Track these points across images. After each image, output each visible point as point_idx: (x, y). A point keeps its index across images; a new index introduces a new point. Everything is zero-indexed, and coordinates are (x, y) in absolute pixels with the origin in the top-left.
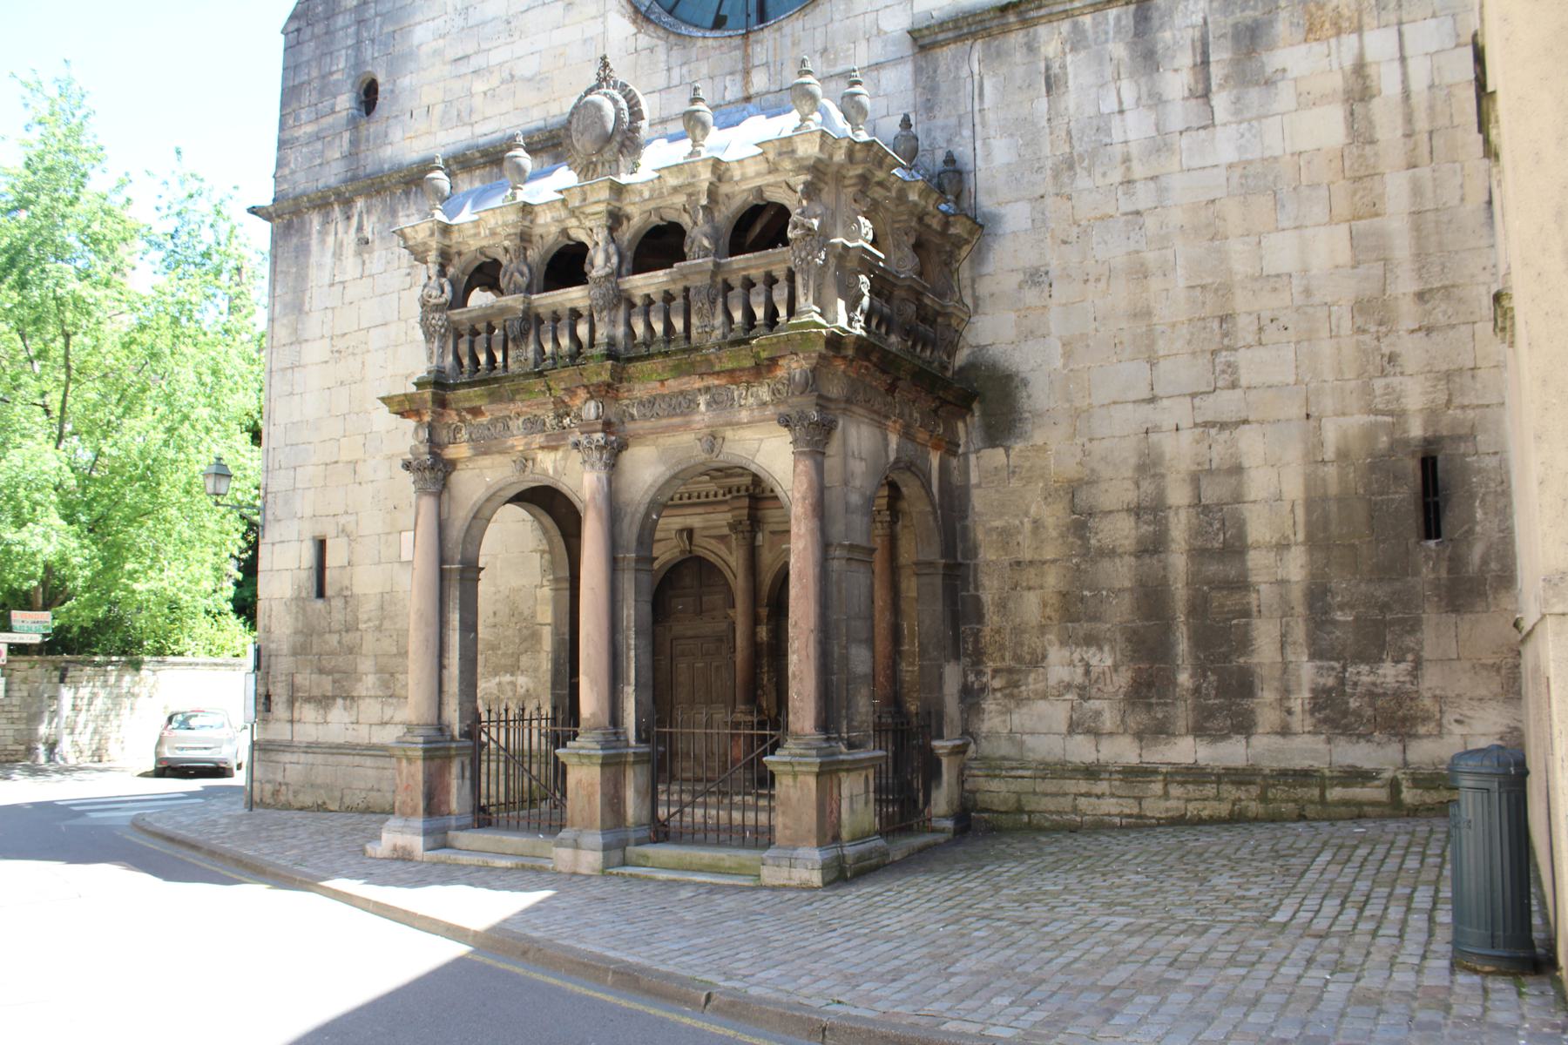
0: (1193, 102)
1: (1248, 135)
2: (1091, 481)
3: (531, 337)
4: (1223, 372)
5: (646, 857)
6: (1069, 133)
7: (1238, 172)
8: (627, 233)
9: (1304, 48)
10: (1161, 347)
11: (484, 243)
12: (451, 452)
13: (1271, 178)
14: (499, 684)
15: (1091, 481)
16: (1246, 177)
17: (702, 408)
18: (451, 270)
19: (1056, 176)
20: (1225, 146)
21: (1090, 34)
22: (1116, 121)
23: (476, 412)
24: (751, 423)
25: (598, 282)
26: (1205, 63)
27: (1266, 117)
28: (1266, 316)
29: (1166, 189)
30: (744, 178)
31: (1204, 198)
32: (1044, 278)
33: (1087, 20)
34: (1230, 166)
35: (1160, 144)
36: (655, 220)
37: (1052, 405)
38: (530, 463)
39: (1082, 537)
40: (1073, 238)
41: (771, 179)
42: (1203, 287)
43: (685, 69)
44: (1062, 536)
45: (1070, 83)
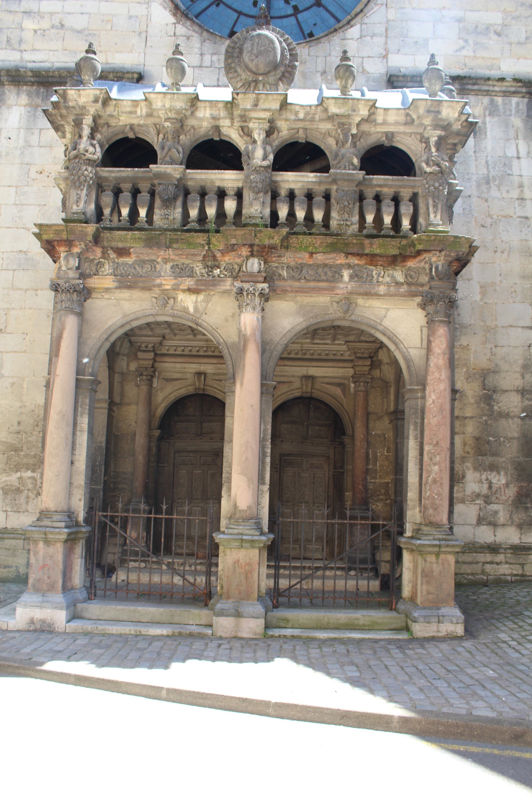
2: (495, 371)
5: (287, 620)
6: (487, 162)
8: (278, 140)
11: (135, 122)
12: (94, 282)
14: (20, 478)
15: (495, 371)
17: (346, 278)
18: (98, 136)
19: (479, 186)
21: (501, 108)
22: (515, 162)
23: (122, 252)
24: (388, 295)
25: (257, 170)
30: (385, 123)
33: (499, 100)
36: (301, 137)
37: (473, 322)
38: (172, 301)
39: (489, 405)
40: (488, 224)
41: (402, 129)
44: (477, 403)
45: (488, 134)
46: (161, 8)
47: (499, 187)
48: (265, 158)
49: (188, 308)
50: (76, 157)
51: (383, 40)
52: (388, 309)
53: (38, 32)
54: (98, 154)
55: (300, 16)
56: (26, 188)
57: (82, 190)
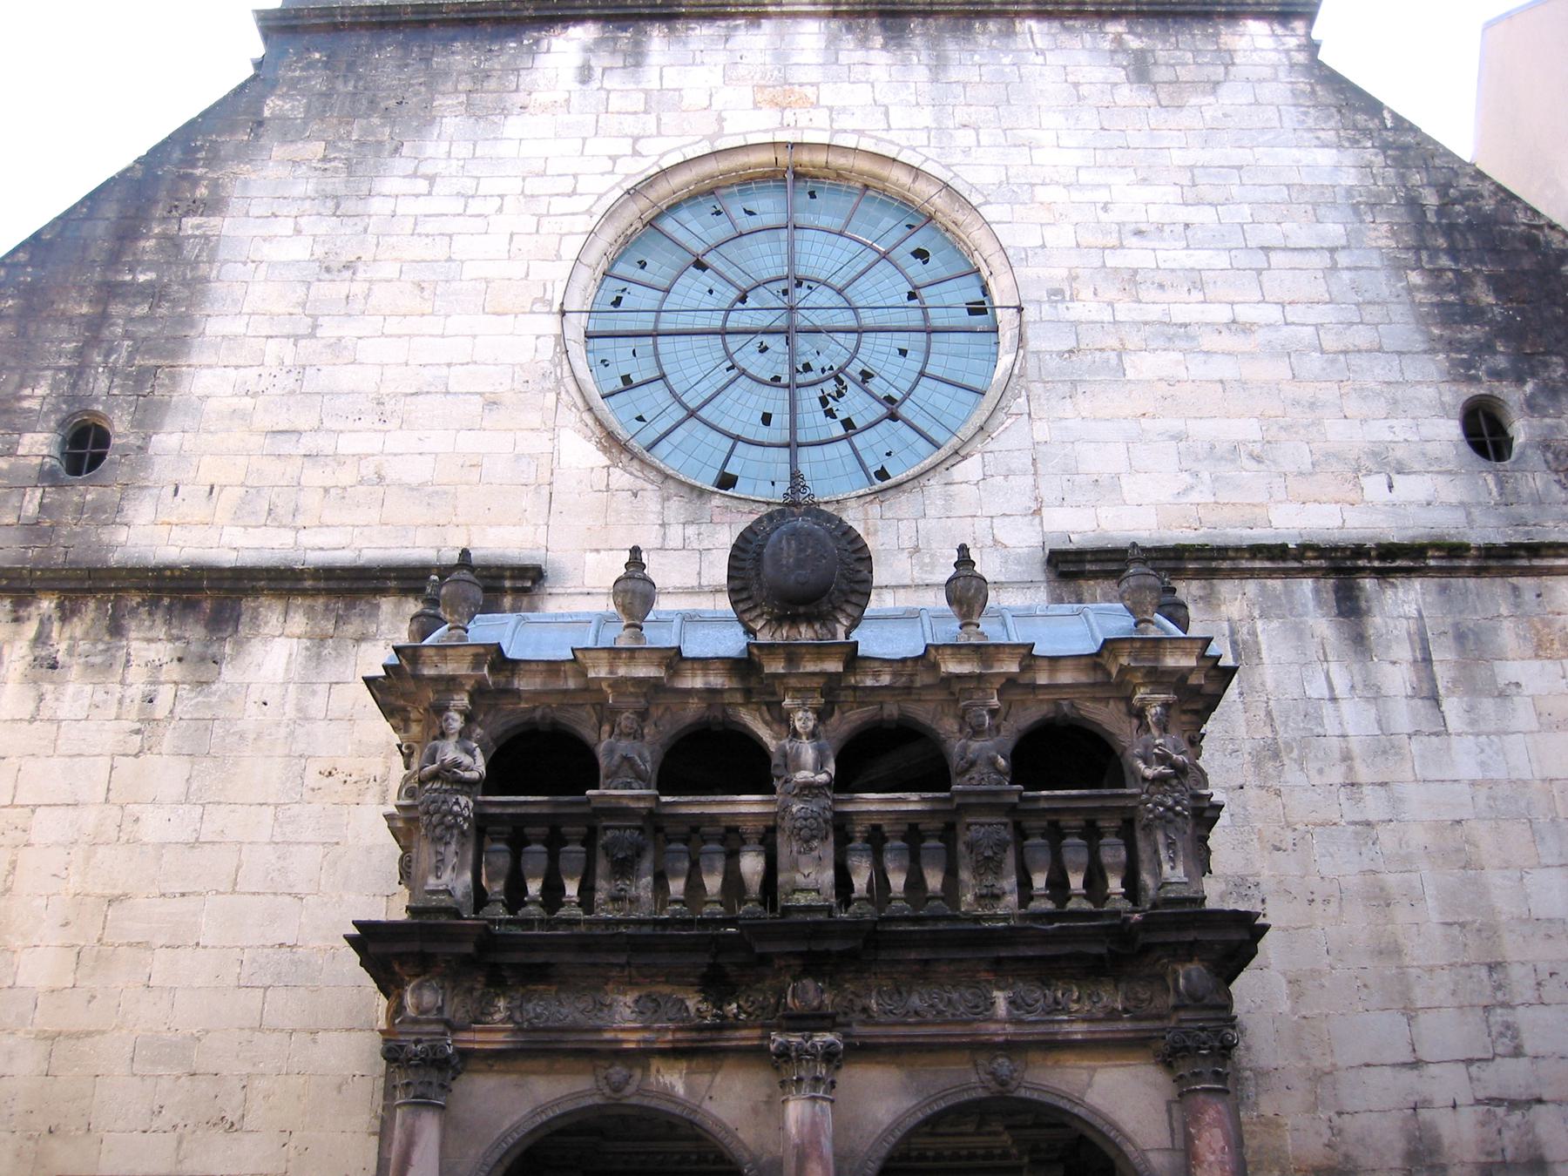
0: (1420, 702)
1: (1487, 749)
3: (647, 864)
4: (1502, 1035)
6: (1269, 713)
7: (1483, 792)
9: (1537, 664)
10: (1420, 997)
13: (1523, 804)
16: (1495, 799)
19: (1258, 765)
20: (1465, 759)
26: (1427, 660)
27: (1507, 733)
28: (1544, 968)
29: (1401, 800)
31: (1448, 817)
32: (1253, 890)
34: (1473, 783)
35: (1385, 745)
37: (1281, 1063)
42: (1462, 925)
43: (691, 531)
45: (1264, 654)
46: (579, 438)
47: (1300, 762)
48: (819, 766)
49: (673, 1087)
50: (435, 776)
51: (1030, 480)
52: (1094, 1069)
53: (332, 491)
54: (477, 766)
55: (857, 440)
56: (296, 808)
57: (447, 844)
